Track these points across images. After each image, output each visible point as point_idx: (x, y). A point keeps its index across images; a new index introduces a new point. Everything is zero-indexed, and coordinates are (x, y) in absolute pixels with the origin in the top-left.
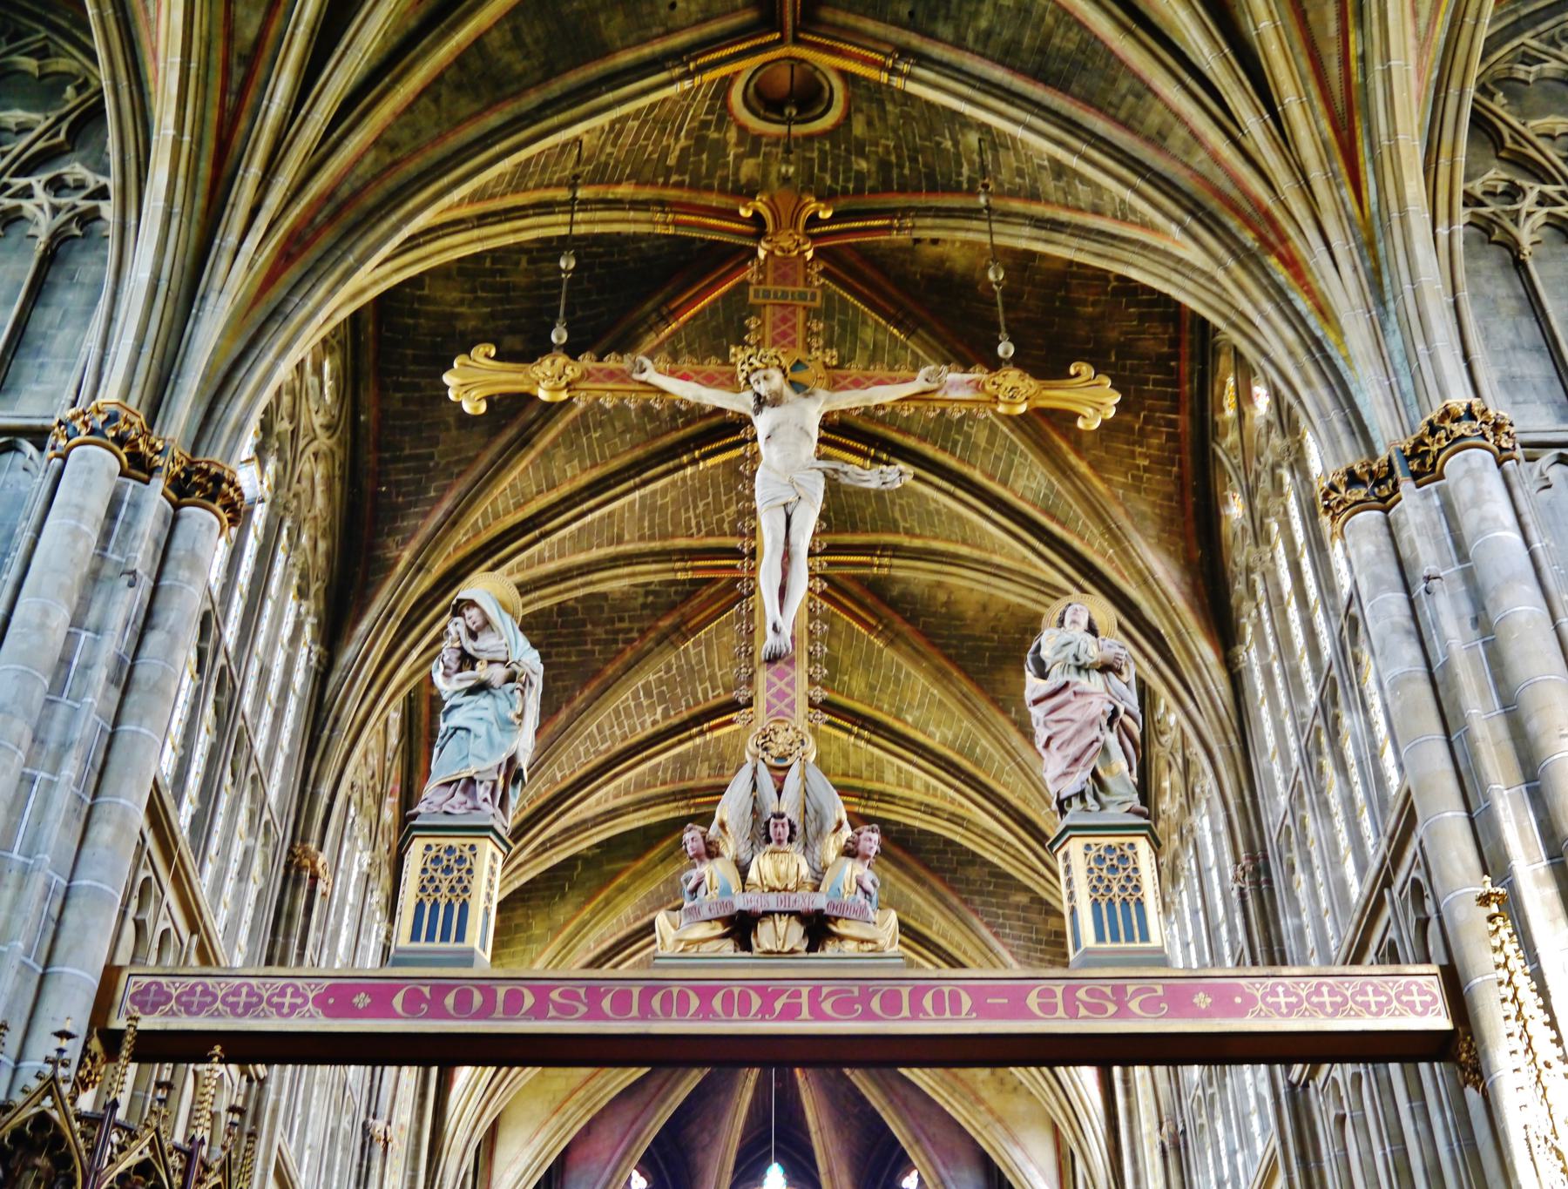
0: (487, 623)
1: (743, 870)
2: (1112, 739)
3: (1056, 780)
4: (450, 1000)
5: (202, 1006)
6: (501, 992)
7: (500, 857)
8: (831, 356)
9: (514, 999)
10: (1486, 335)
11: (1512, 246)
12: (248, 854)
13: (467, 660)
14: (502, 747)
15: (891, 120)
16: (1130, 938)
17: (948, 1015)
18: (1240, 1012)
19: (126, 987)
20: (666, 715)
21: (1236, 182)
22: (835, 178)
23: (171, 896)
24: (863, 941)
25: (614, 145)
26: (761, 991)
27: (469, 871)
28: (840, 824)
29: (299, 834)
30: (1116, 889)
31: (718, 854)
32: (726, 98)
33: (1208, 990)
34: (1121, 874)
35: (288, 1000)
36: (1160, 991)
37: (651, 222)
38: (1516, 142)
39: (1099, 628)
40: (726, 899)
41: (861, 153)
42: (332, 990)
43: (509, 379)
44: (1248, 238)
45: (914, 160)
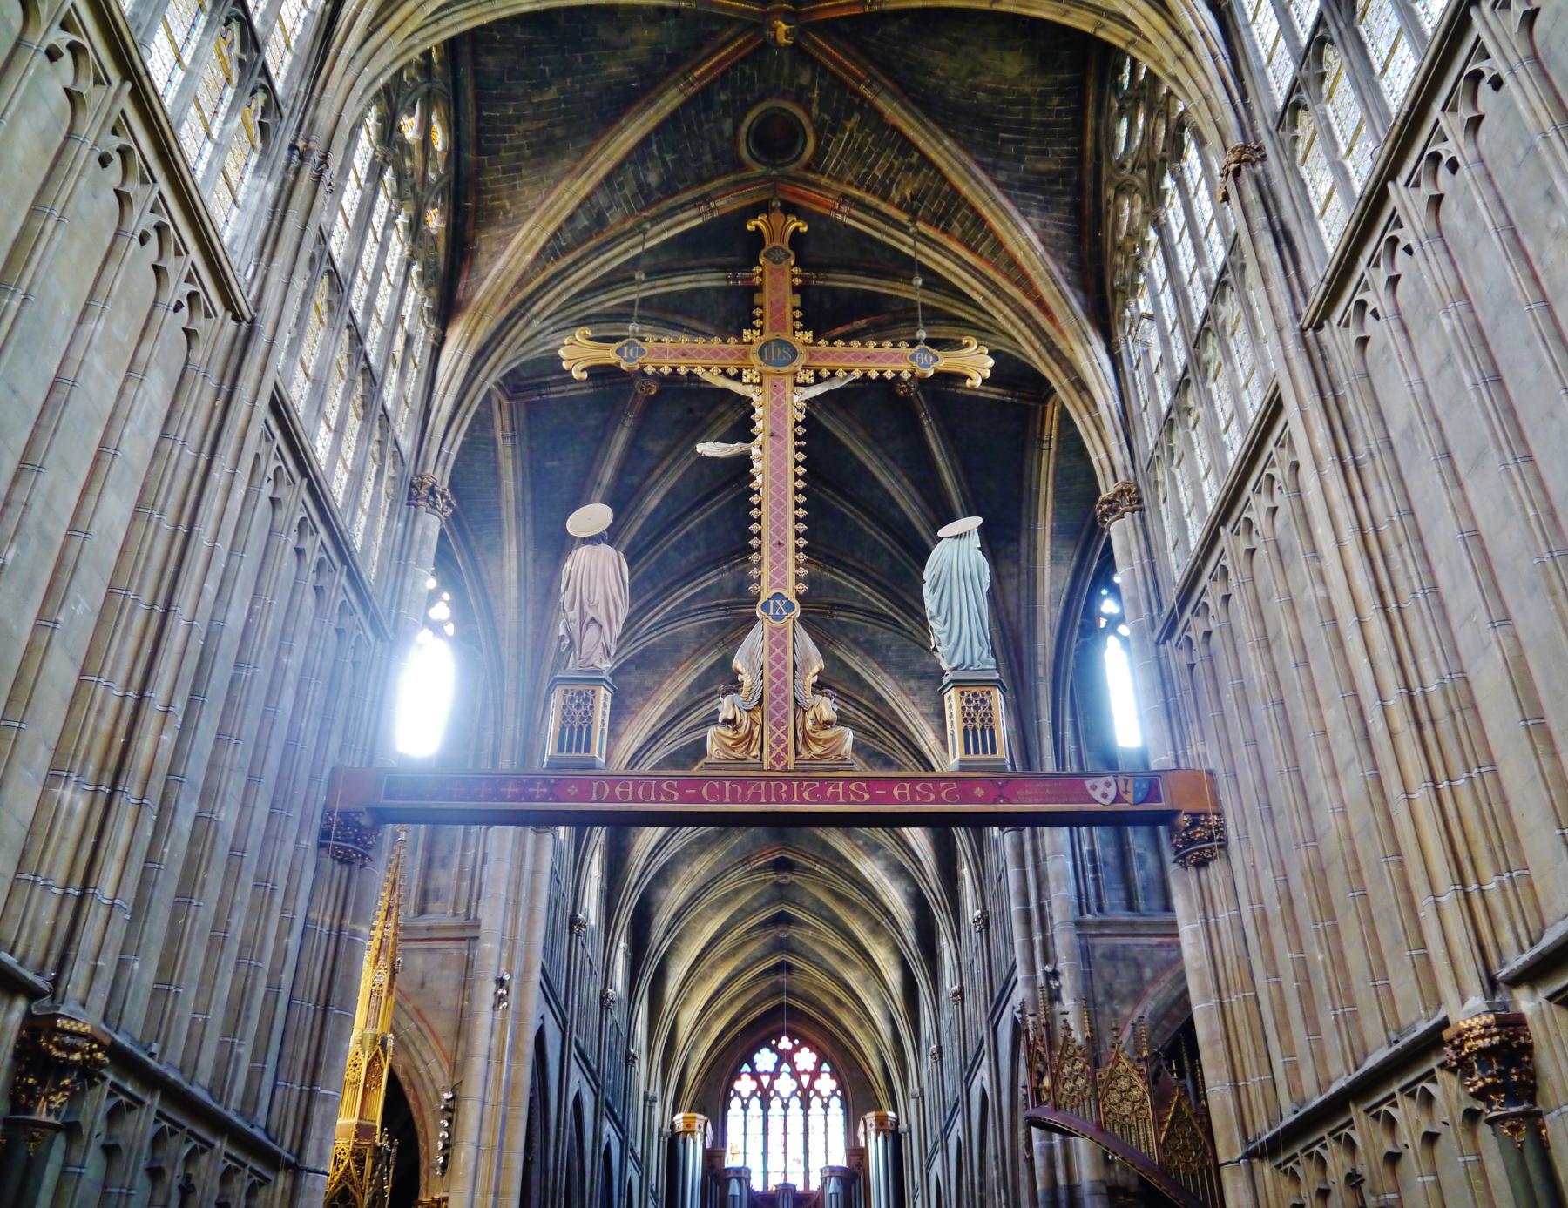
15: (707, 148)
22: (743, 72)
25: (892, 165)
32: (817, 146)
41: (724, 104)
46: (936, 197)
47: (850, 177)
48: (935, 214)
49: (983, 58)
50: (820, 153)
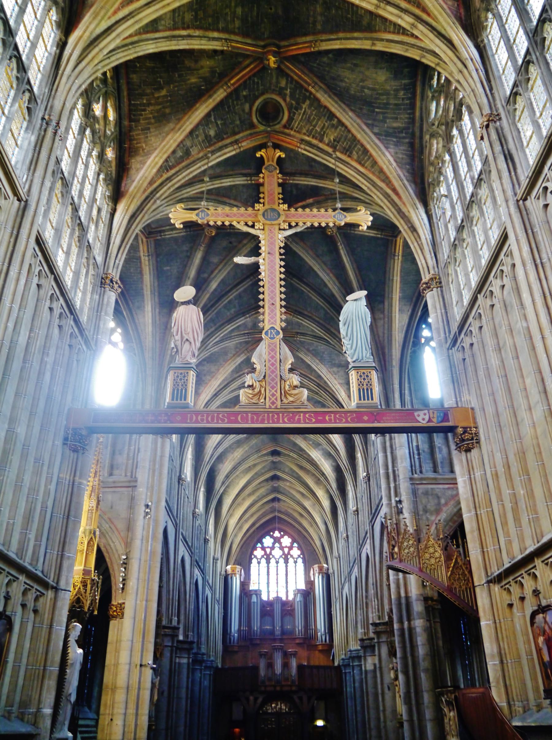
15: (237, 118)
22: (254, 81)
25: (324, 125)
32: (289, 116)
41: (245, 97)
45: (229, 107)
46: (345, 140)
47: (304, 131)
48: (344, 148)
49: (367, 73)
50: (291, 119)
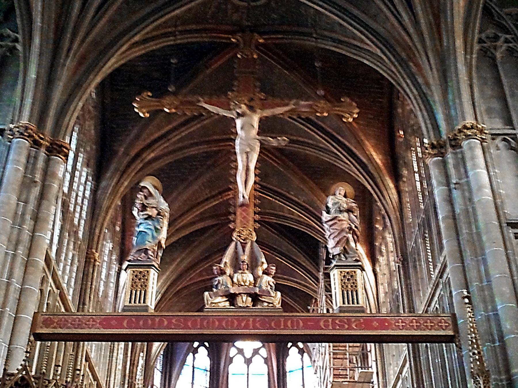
0: (151, 194)
1: (231, 278)
2: (350, 236)
3: (332, 249)
4: (141, 323)
5: (65, 325)
6: (157, 320)
7: (156, 274)
8: (262, 96)
9: (161, 322)
10: (482, 91)
11: (494, 59)
12: (73, 256)
13: (144, 208)
14: (156, 238)
16: (353, 303)
17: (295, 328)
18: (386, 328)
19: (40, 319)
20: (210, 192)
21: (399, 34)
23: (51, 280)
24: (269, 303)
26: (238, 320)
27: (147, 280)
28: (263, 263)
29: (90, 247)
30: (350, 287)
31: (225, 273)
33: (377, 321)
34: (351, 281)
35: (91, 323)
36: (362, 321)
37: (202, 37)
38: (499, 18)
39: (348, 195)
40: (227, 289)
42: (104, 320)
43: (154, 104)
44: (403, 55)
